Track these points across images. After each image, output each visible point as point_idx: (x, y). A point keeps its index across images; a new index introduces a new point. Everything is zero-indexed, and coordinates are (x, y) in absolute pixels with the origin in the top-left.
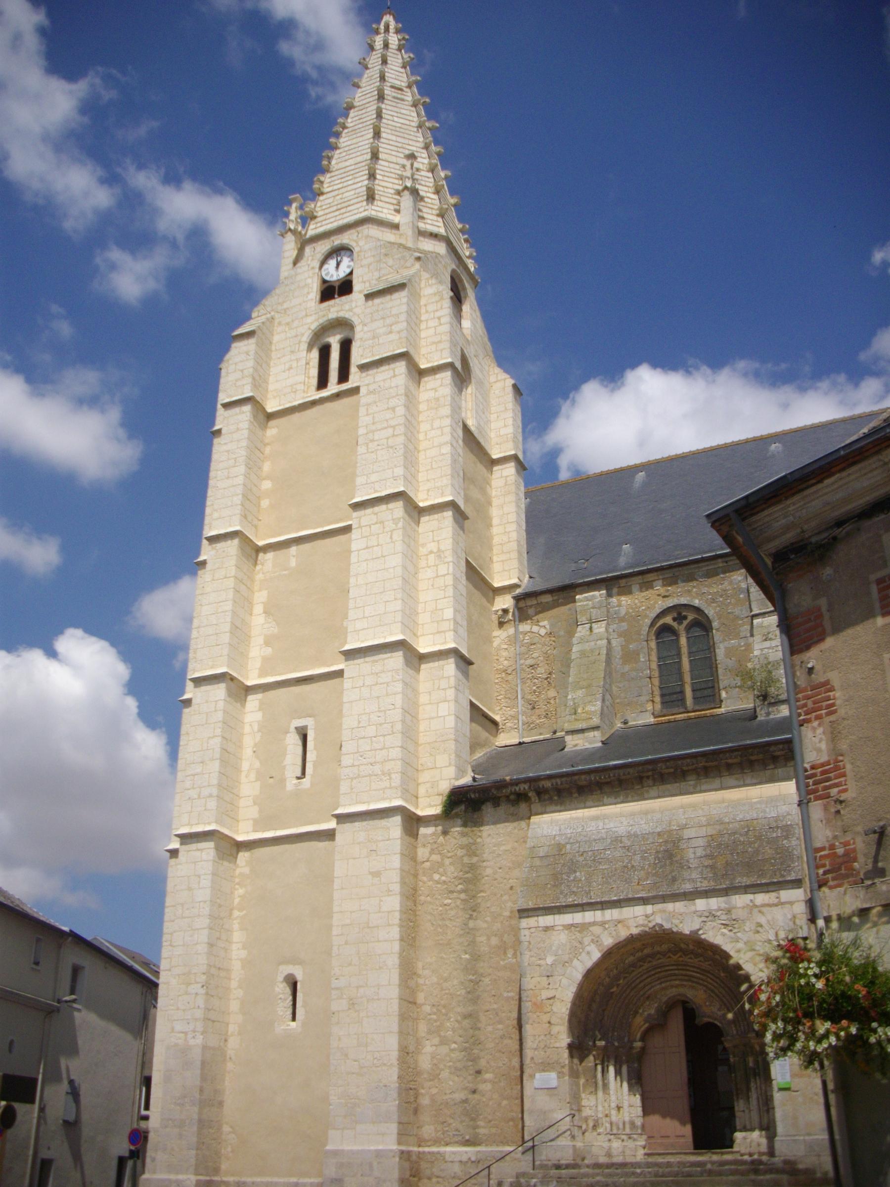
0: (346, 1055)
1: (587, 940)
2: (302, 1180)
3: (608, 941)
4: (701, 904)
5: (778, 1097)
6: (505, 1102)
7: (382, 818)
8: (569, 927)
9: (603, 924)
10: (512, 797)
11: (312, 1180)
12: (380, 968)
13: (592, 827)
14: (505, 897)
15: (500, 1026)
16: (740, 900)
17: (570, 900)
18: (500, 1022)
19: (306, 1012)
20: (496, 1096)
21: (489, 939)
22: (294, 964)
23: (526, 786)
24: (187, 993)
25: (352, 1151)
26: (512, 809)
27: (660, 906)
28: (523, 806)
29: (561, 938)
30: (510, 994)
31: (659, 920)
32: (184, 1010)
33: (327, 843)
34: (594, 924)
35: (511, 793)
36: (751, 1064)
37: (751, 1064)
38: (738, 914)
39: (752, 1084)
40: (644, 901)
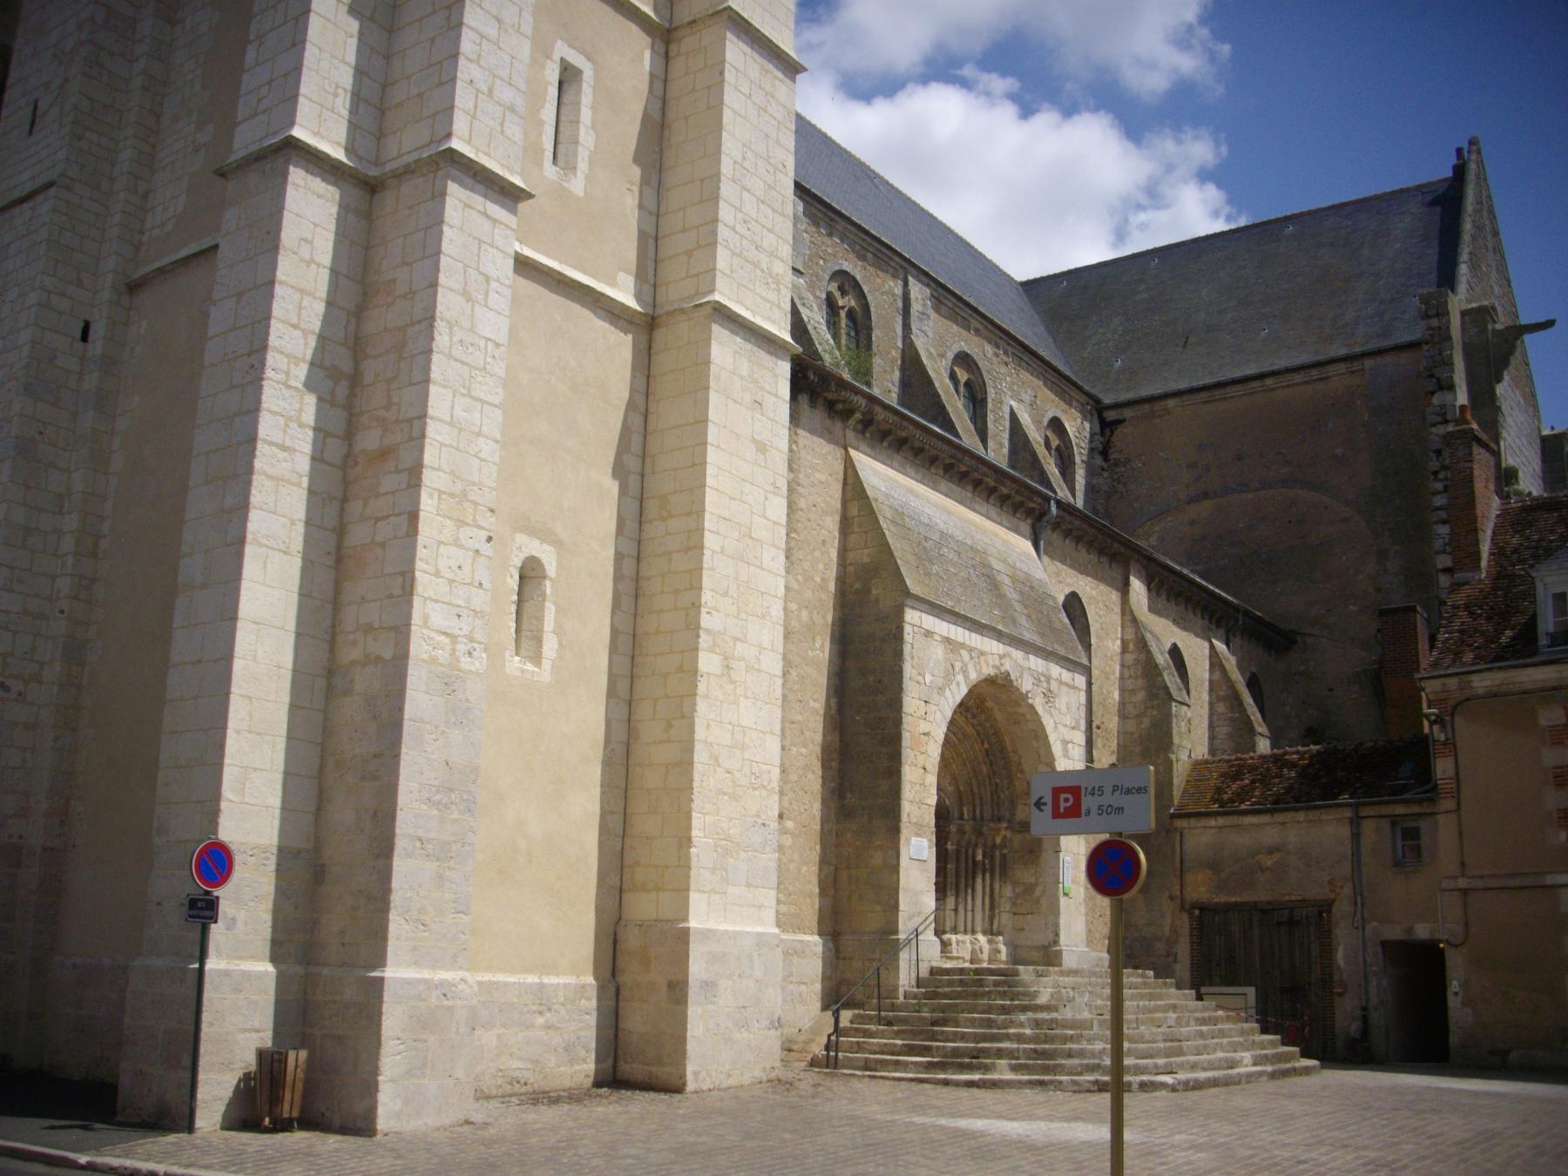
0: (716, 759)
1: (958, 665)
2: (546, 980)
3: (974, 676)
4: (1036, 663)
5: (1063, 900)
6: (804, 869)
7: (769, 352)
8: (947, 640)
9: (971, 650)
10: (839, 407)
11: (561, 980)
12: (763, 617)
13: (914, 503)
14: (817, 553)
15: (804, 751)
16: (1056, 670)
17: (949, 604)
18: (805, 746)
19: (560, 644)
20: (796, 857)
21: (799, 610)
22: (543, 541)
23: (863, 402)
24: (457, 543)
25: (727, 932)
26: (828, 422)
27: (1009, 649)
28: (839, 425)
29: (938, 652)
30: (817, 705)
31: (1007, 666)
32: (451, 582)
33: (607, 325)
34: (963, 646)
35: (844, 402)
36: (979, 857)
37: (979, 857)
38: (1054, 686)
39: (979, 880)
40: (999, 636)
